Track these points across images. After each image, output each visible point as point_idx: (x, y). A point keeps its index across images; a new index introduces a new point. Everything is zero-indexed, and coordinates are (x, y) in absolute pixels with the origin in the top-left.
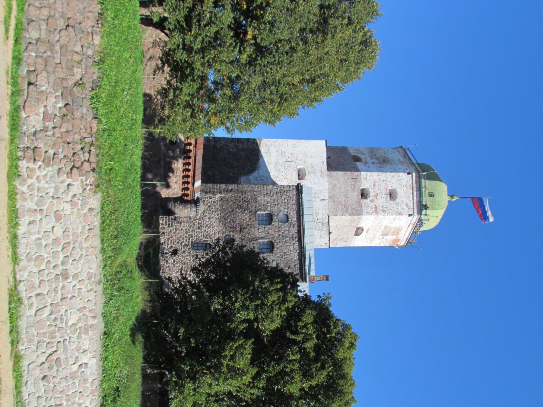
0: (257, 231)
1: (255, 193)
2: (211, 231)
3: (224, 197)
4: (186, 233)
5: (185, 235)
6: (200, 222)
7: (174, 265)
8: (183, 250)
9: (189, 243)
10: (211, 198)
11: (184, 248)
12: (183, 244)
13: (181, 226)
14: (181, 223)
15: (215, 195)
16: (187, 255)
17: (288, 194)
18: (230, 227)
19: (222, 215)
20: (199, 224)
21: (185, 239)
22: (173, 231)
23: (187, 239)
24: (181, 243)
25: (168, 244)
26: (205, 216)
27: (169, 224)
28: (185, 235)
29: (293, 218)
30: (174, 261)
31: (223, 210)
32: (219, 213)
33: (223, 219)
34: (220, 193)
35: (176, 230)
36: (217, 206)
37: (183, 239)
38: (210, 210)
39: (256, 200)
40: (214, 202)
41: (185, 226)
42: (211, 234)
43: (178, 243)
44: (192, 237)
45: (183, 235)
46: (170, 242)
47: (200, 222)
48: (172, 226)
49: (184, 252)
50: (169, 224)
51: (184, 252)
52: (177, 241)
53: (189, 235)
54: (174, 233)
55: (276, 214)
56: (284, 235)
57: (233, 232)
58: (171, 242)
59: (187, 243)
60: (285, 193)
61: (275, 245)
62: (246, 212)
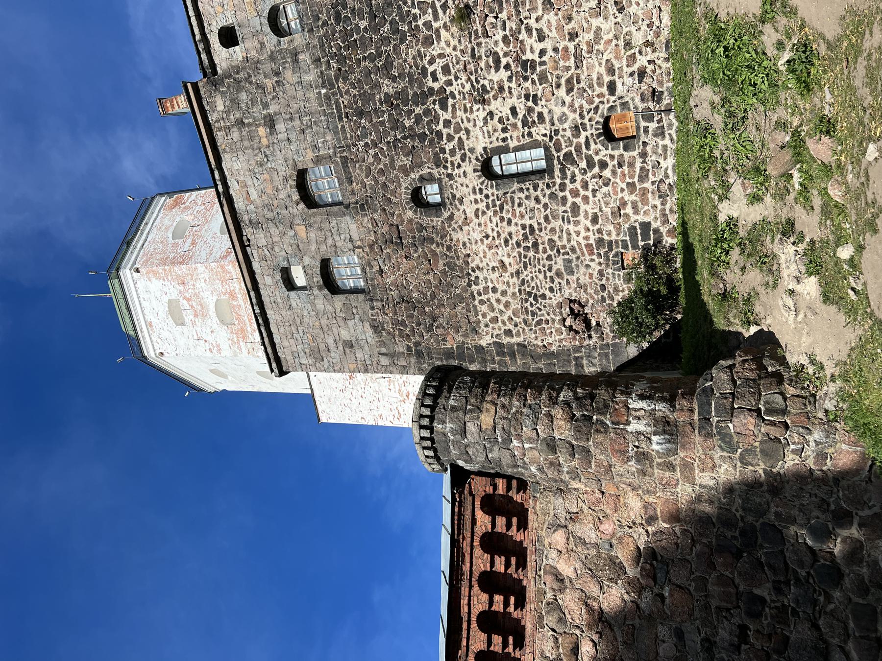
0: (355, 237)
1: (384, 350)
2: (490, 223)
3: (466, 336)
4: (575, 209)
5: (578, 200)
6: (531, 253)
7: (611, 71)
8: (582, 140)
9: (563, 170)
10: (508, 333)
11: (578, 149)
12: (583, 164)
13: (600, 231)
14: (600, 242)
15: (495, 343)
16: (563, 118)
17: (300, 348)
18: (431, 240)
19: (464, 283)
20: (535, 245)
21: (578, 185)
22: (629, 210)
23: (570, 186)
24: (591, 164)
25: (644, 155)
26: (518, 273)
27: (646, 236)
28: (578, 200)
29: (269, 282)
30: (612, 87)
31: (466, 299)
32: (473, 287)
33: (458, 268)
34: (480, 349)
35: (617, 212)
36: (484, 308)
37: (585, 186)
38: (504, 293)
39: (377, 328)
40: (495, 320)
41: (581, 233)
42: (490, 213)
43: (603, 165)
44: (553, 196)
45: (586, 199)
46: (638, 165)
47: (531, 253)
48: (632, 230)
49: (577, 130)
50: (646, 236)
51: (577, 130)
52: (607, 173)
53: (564, 200)
54: (624, 204)
55: (316, 291)
56: (281, 227)
57: (421, 228)
58: (631, 165)
59: (571, 169)
60: (307, 351)
61: (296, 197)
62: (395, 293)
